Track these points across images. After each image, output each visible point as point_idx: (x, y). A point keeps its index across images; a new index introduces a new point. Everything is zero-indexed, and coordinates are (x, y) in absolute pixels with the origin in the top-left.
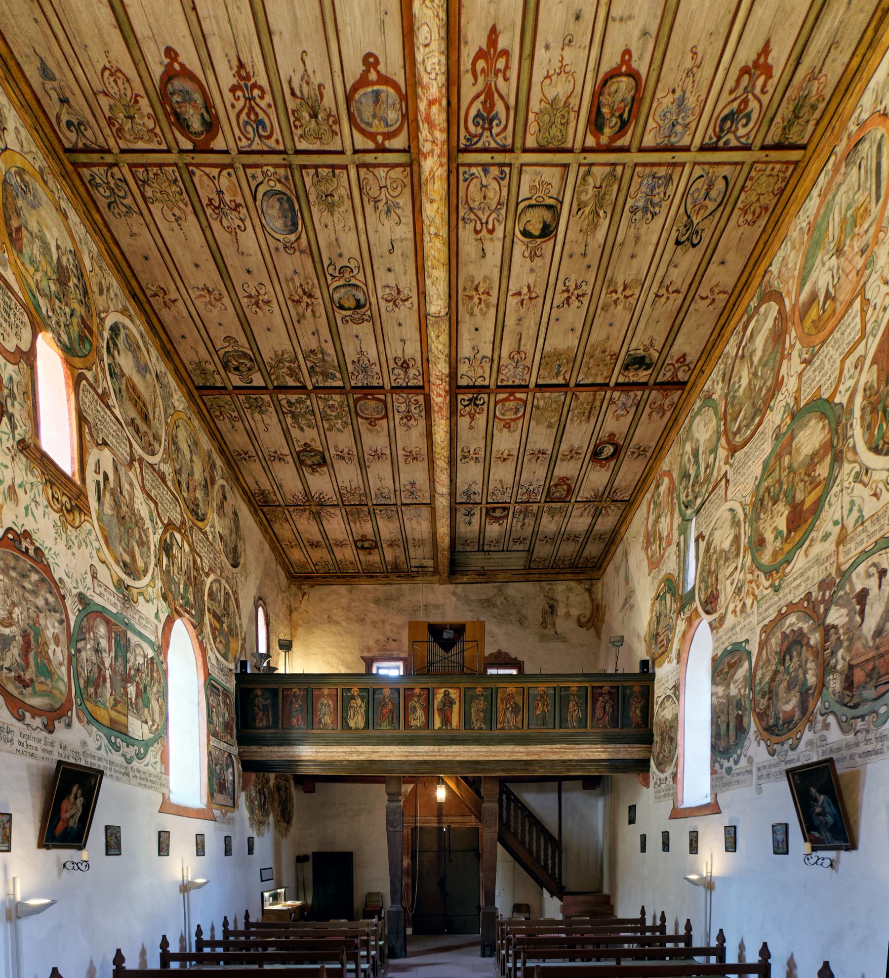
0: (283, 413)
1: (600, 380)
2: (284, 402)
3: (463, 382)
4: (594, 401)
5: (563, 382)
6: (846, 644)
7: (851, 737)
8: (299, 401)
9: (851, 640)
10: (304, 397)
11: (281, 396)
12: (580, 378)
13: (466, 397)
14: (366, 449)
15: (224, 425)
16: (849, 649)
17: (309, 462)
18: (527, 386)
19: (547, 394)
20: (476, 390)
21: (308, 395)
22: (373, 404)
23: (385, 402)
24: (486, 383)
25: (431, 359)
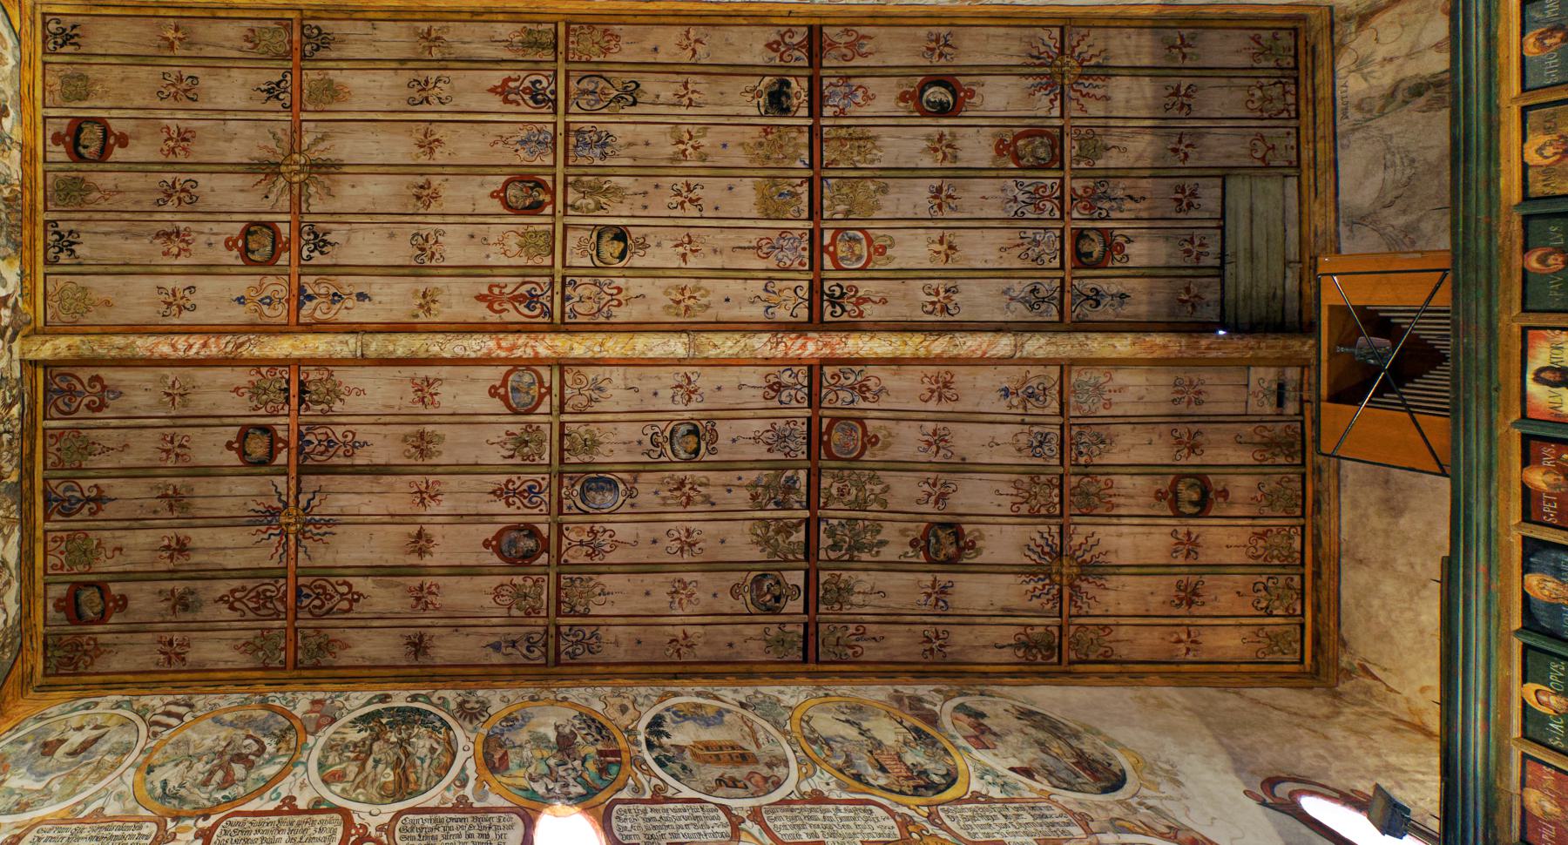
0: (851, 560)
1: (805, 139)
2: (833, 555)
3: (803, 314)
4: (838, 138)
5: (806, 185)
8: (832, 533)
10: (823, 526)
11: (822, 555)
12: (798, 164)
13: (828, 309)
14: (922, 457)
15: (871, 652)
17: (952, 550)
18: (811, 231)
19: (826, 203)
20: (816, 298)
21: (819, 520)
22: (837, 436)
23: (834, 420)
24: (806, 284)
25: (747, 354)
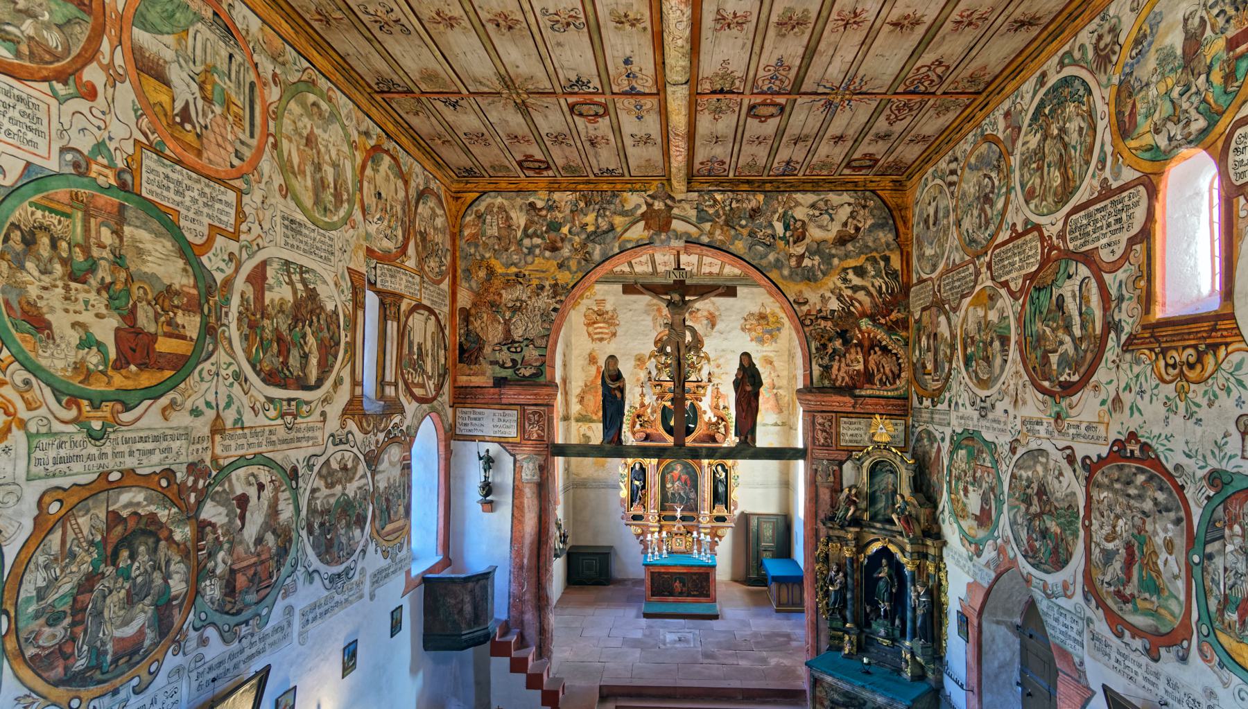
6: (226, 546)
7: (235, 646)
9: (232, 543)
16: (231, 552)
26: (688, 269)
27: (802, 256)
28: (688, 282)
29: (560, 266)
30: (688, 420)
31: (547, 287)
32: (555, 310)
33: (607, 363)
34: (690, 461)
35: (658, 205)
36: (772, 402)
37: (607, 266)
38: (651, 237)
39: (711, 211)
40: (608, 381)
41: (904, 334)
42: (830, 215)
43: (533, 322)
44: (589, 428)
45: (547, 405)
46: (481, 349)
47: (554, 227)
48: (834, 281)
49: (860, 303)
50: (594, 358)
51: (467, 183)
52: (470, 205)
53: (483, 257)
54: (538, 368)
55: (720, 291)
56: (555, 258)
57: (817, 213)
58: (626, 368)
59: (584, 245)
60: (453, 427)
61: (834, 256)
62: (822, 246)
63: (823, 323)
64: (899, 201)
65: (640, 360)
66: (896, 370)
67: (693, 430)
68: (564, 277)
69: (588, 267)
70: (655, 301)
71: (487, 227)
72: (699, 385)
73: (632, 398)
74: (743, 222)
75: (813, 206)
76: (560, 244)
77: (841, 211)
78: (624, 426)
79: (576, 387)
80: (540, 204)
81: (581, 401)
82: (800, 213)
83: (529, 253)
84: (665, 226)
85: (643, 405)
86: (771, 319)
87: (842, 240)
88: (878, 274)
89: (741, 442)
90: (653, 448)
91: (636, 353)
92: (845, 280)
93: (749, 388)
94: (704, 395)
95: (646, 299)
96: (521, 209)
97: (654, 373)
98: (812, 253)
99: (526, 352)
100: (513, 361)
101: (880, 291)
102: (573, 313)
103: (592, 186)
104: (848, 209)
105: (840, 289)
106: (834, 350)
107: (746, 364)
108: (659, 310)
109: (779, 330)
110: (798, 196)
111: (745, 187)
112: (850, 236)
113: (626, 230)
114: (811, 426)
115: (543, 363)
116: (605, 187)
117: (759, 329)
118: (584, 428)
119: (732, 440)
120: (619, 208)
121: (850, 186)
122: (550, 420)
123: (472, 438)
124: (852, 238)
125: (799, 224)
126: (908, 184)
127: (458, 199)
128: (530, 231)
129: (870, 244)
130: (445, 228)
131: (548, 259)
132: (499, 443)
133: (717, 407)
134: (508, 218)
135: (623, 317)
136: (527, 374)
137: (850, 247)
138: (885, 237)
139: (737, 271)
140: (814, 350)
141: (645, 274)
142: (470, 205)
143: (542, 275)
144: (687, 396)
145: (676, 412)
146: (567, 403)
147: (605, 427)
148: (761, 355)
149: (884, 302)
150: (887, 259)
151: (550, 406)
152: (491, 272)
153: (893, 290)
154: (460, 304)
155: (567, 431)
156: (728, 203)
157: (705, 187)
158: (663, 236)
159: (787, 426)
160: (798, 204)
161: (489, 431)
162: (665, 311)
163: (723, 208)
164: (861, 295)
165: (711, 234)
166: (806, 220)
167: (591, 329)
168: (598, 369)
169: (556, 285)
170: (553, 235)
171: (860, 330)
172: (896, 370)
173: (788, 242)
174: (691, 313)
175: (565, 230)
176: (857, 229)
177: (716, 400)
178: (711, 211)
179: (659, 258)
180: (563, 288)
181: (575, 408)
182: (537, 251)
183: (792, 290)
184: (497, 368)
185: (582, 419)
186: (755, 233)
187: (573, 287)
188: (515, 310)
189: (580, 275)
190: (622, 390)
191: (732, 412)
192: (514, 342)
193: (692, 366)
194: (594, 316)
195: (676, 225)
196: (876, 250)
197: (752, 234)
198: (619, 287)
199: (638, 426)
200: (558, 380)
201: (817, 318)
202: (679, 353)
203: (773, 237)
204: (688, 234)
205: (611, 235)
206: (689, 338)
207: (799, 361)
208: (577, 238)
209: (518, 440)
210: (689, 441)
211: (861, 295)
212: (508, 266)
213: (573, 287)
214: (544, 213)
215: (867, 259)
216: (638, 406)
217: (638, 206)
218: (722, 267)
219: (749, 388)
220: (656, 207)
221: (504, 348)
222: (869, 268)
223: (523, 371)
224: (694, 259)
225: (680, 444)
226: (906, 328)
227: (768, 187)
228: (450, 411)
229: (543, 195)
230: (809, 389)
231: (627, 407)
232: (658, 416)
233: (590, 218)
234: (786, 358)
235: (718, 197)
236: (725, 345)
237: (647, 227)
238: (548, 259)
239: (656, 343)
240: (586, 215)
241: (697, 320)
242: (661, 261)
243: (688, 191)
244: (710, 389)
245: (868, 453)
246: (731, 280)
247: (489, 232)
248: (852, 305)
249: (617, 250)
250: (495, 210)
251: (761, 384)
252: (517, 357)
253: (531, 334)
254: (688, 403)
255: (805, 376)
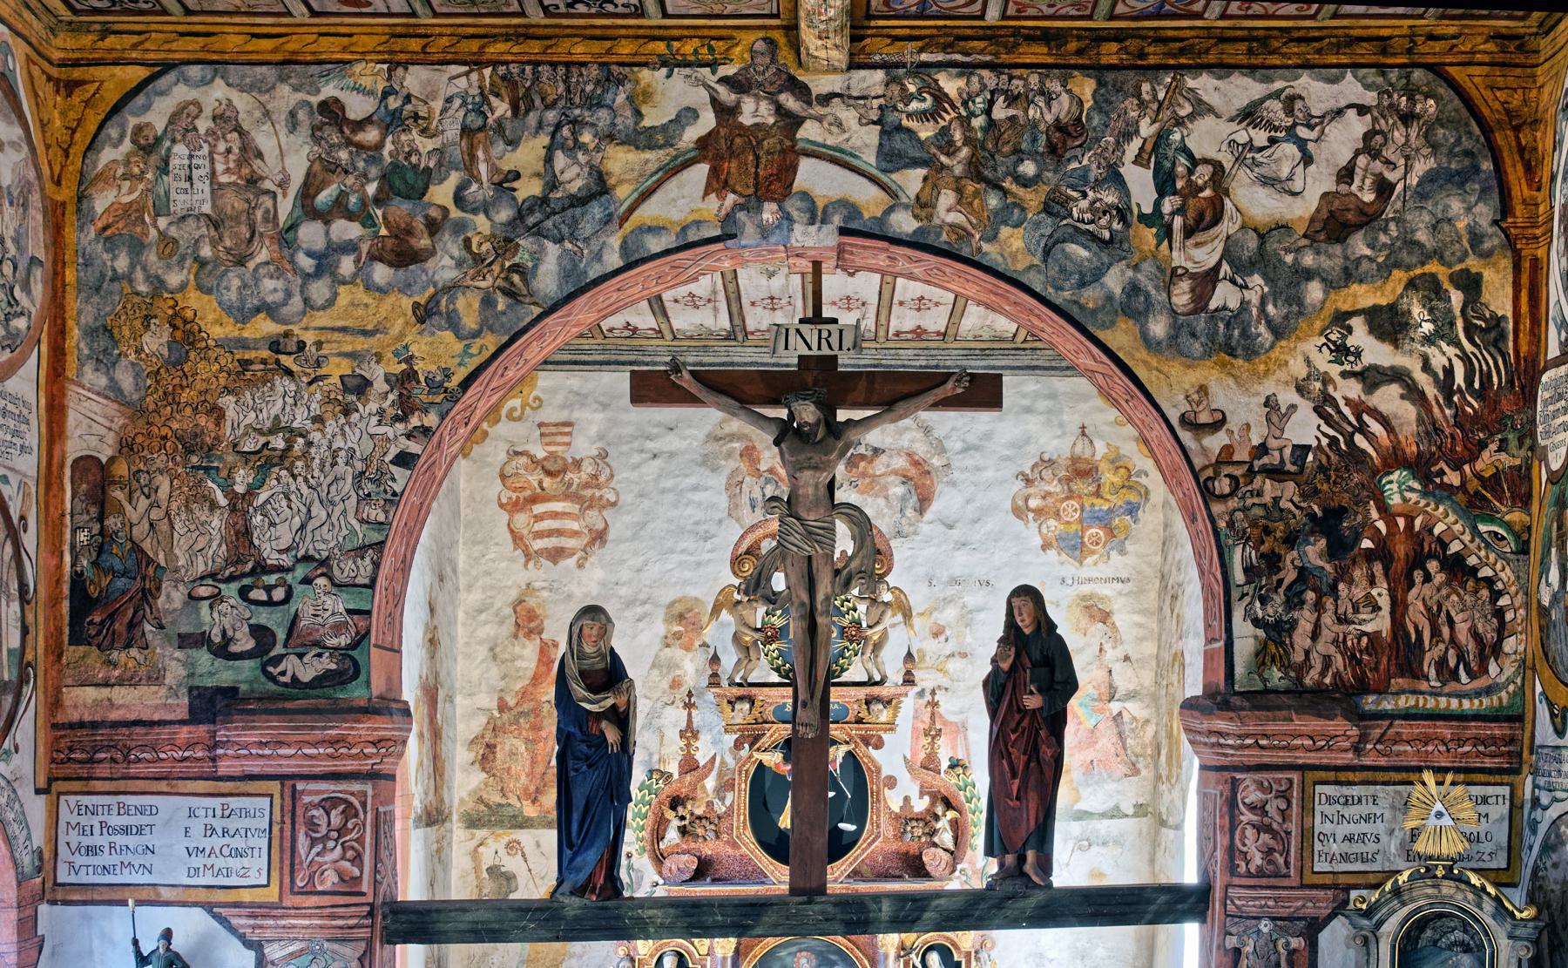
26: (847, 319)
27: (1208, 279)
28: (847, 361)
29: (424, 314)
30: (837, 810)
31: (380, 385)
32: (404, 460)
33: (576, 636)
34: (840, 941)
35: (755, 111)
36: (1107, 741)
37: (582, 312)
38: (728, 219)
39: (926, 132)
40: (579, 691)
41: (1516, 517)
42: (1302, 144)
43: (327, 503)
44: (512, 846)
45: (373, 776)
46: (147, 595)
47: (406, 182)
48: (1308, 352)
49: (1385, 421)
50: (532, 615)
51: (105, 32)
52: (116, 109)
53: (158, 284)
54: (342, 653)
55: (949, 388)
56: (406, 288)
57: (1260, 137)
58: (635, 645)
59: (505, 244)
60: (46, 861)
61: (1309, 275)
62: (1272, 245)
63: (1269, 488)
64: (1516, 101)
65: (684, 618)
66: (1488, 631)
67: (853, 840)
68: (437, 351)
69: (517, 311)
70: (736, 425)
71: (173, 183)
72: (874, 692)
73: (656, 745)
74: (1028, 168)
75: (1249, 115)
76: (424, 242)
77: (1333, 130)
78: (629, 835)
79: (467, 717)
80: (358, 106)
81: (486, 758)
82: (1206, 137)
83: (318, 273)
84: (774, 181)
85: (689, 765)
86: (1109, 477)
87: (1335, 224)
88: (1443, 332)
89: (1005, 874)
90: (723, 904)
91: (669, 595)
92: (1341, 351)
93: (1033, 702)
94: (890, 726)
95: (708, 418)
96: (293, 125)
97: (729, 659)
98: (1239, 264)
99: (304, 604)
100: (259, 632)
101: (1446, 382)
102: (462, 465)
103: (535, 47)
104: (1356, 126)
105: (1326, 380)
106: (1303, 573)
107: (1026, 623)
108: (749, 454)
109: (1132, 510)
110: (1204, 84)
111: (1037, 53)
112: (1362, 209)
113: (646, 195)
114: (1226, 811)
115: (361, 639)
116: (580, 50)
117: (1071, 509)
118: (494, 848)
119: (977, 869)
120: (625, 120)
121: (1364, 52)
122: (382, 825)
123: (112, 896)
124: (1368, 218)
125: (1203, 174)
126: (1544, 44)
127: (71, 86)
128: (324, 197)
129: (1422, 236)
130: (26, 187)
131: (383, 291)
132: (209, 907)
133: (930, 764)
134: (250, 153)
135: (627, 478)
136: (306, 676)
137: (1359, 245)
138: (1467, 212)
139: (1004, 325)
140: (1239, 576)
141: (703, 339)
142: (116, 109)
143: (361, 344)
144: (835, 731)
145: (796, 786)
146: (437, 767)
147: (565, 842)
148: (1071, 593)
149: (1460, 420)
150: (1471, 284)
151: (381, 777)
152: (186, 334)
153: (1486, 379)
154: (74, 448)
155: (438, 857)
156: (979, 103)
157: (909, 53)
158: (769, 213)
159: (1156, 818)
160: (1202, 108)
161: (172, 870)
162: (770, 457)
163: (965, 122)
164: (1389, 398)
165: (923, 205)
166: (1227, 160)
167: (521, 519)
168: (544, 650)
169: (410, 376)
170: (401, 209)
171: (1384, 509)
172: (1488, 631)
173: (1167, 232)
174: (852, 463)
175: (441, 194)
176: (1384, 189)
177: (927, 738)
178: (926, 132)
179: (752, 282)
180: (433, 386)
181: (465, 782)
182: (347, 265)
183: (1175, 386)
184: (203, 657)
185: (485, 817)
186: (1065, 202)
187: (466, 384)
188: (265, 463)
189: (490, 342)
190: (622, 719)
191: (980, 777)
192: (262, 568)
193: (854, 633)
194: (534, 478)
195: (812, 176)
196: (1438, 254)
197: (1055, 206)
198: (620, 381)
199: (672, 835)
200: (410, 692)
201: (1251, 473)
202: (811, 594)
203: (1122, 214)
204: (851, 209)
205: (596, 210)
206: (844, 543)
207: (1193, 608)
208: (481, 222)
209: (272, 894)
210: (838, 877)
211: (1389, 398)
212: (243, 315)
213: (466, 384)
214: (371, 135)
215: (1411, 284)
216: (673, 768)
217: (689, 114)
218: (956, 313)
219: (1033, 702)
220: (746, 119)
221: (231, 590)
222: (1417, 311)
223: (291, 665)
224: (867, 285)
225: (808, 889)
226: (1524, 500)
227: (1110, 53)
228: (37, 808)
229: (371, 75)
230: (1221, 698)
231: (638, 775)
232: (739, 799)
233: (528, 155)
234: (1151, 599)
235: (951, 85)
236: (961, 562)
237: (718, 183)
238: (383, 291)
239: (737, 562)
240: (513, 143)
241: (873, 485)
242: (758, 294)
243: (853, 66)
244: (909, 704)
245: (1397, 892)
246: (985, 353)
247: (180, 203)
248: (1362, 429)
249: (613, 260)
250: (203, 125)
251: (1071, 685)
252: (274, 620)
253: (323, 543)
254: (838, 754)
255: (1208, 657)
